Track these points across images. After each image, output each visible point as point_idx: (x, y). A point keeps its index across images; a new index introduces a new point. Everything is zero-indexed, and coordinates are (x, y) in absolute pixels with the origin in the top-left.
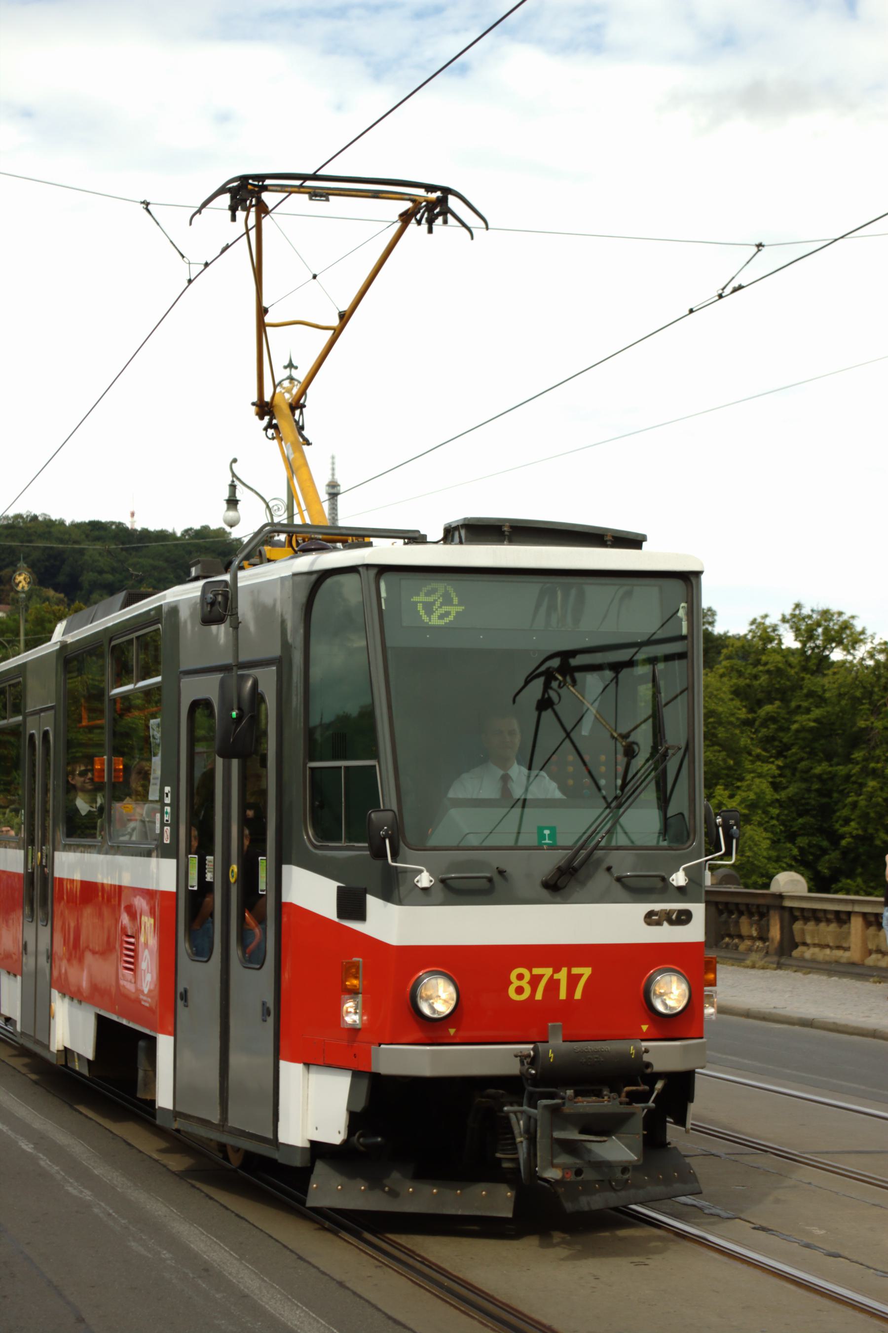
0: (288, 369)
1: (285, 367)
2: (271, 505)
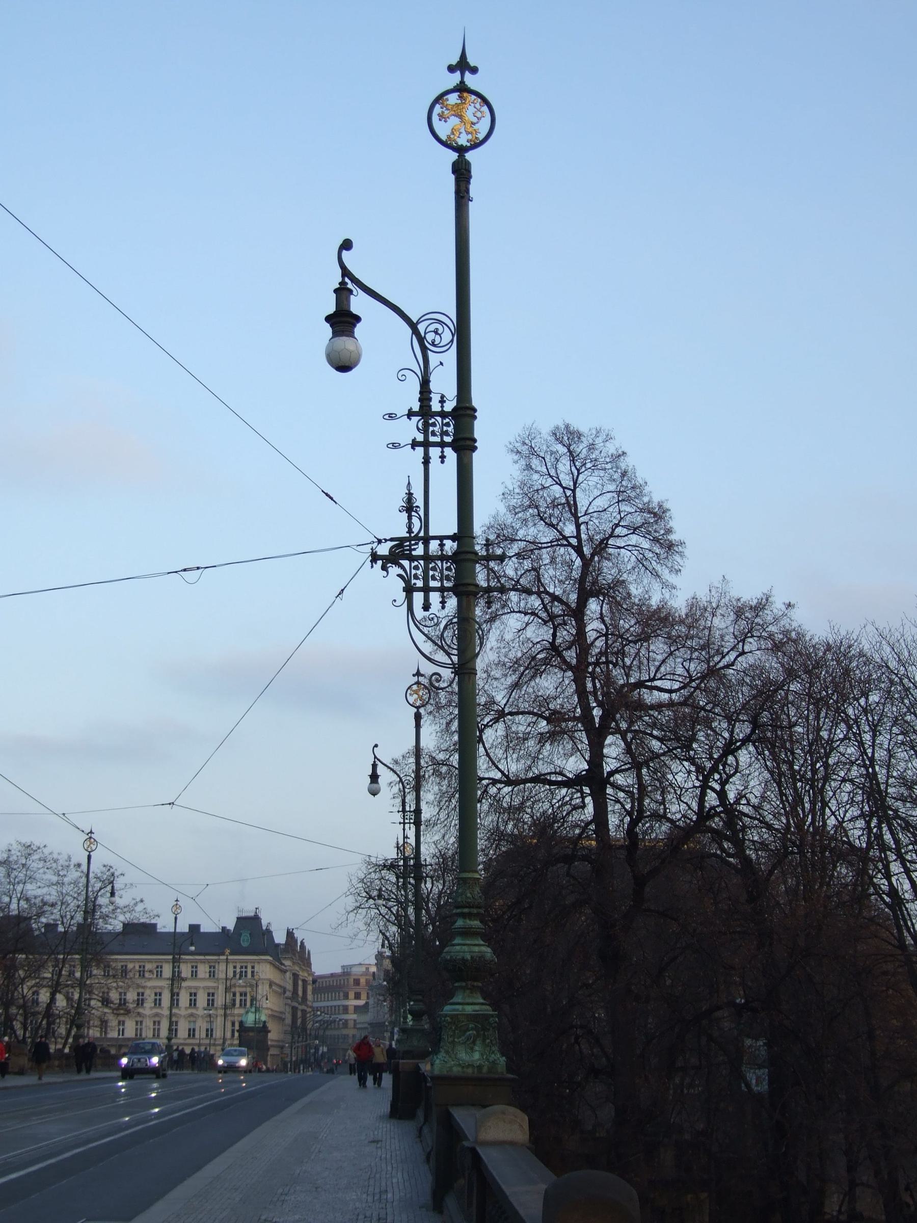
0: (458, 73)
1: (451, 69)
2: (421, 328)
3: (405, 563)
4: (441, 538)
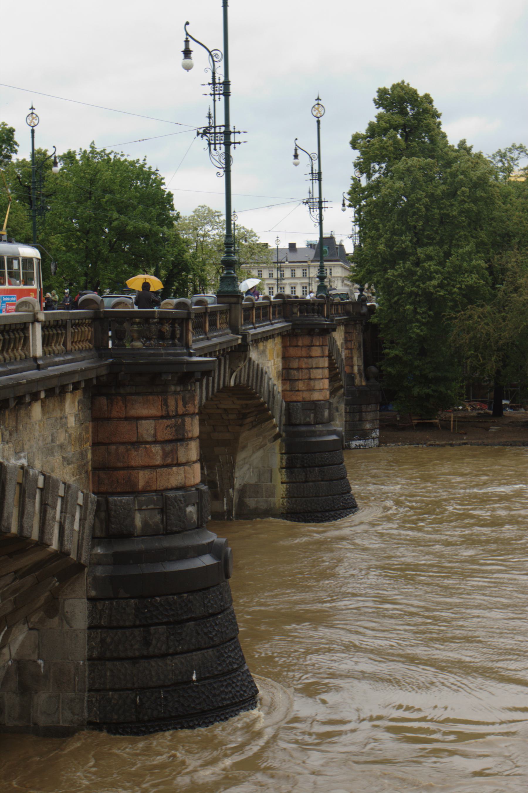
2: (212, 53)
3: (208, 135)
4: (220, 126)
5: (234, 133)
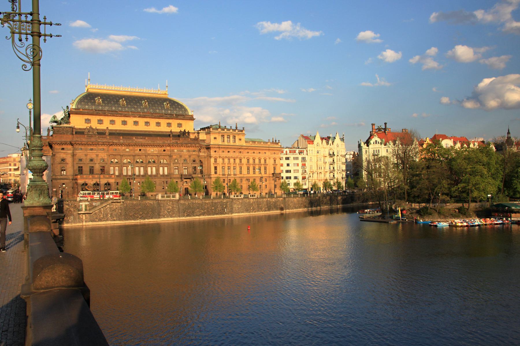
3: (11, 23)
4: (26, 14)
5: (45, 24)
